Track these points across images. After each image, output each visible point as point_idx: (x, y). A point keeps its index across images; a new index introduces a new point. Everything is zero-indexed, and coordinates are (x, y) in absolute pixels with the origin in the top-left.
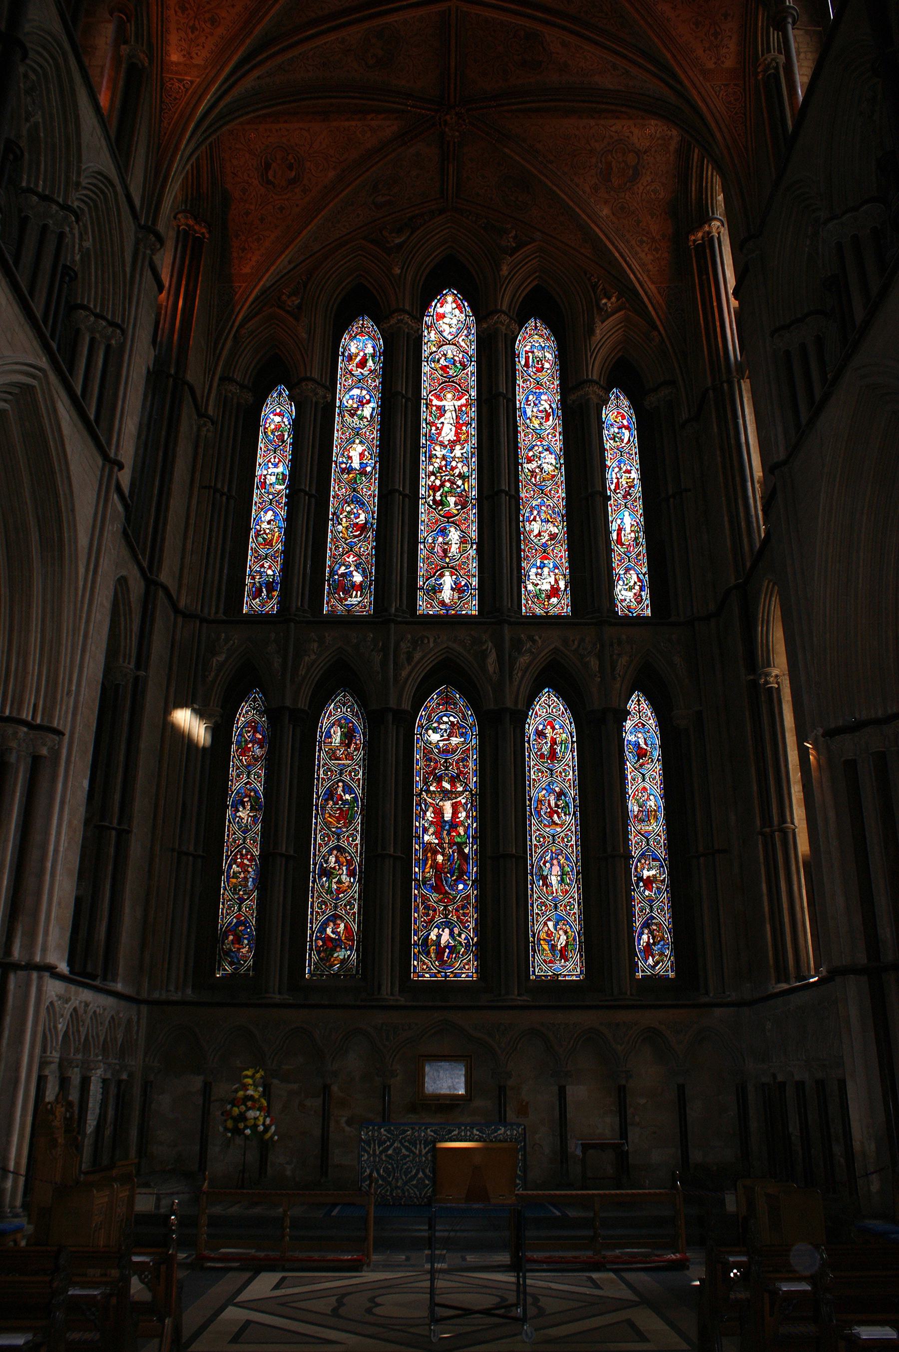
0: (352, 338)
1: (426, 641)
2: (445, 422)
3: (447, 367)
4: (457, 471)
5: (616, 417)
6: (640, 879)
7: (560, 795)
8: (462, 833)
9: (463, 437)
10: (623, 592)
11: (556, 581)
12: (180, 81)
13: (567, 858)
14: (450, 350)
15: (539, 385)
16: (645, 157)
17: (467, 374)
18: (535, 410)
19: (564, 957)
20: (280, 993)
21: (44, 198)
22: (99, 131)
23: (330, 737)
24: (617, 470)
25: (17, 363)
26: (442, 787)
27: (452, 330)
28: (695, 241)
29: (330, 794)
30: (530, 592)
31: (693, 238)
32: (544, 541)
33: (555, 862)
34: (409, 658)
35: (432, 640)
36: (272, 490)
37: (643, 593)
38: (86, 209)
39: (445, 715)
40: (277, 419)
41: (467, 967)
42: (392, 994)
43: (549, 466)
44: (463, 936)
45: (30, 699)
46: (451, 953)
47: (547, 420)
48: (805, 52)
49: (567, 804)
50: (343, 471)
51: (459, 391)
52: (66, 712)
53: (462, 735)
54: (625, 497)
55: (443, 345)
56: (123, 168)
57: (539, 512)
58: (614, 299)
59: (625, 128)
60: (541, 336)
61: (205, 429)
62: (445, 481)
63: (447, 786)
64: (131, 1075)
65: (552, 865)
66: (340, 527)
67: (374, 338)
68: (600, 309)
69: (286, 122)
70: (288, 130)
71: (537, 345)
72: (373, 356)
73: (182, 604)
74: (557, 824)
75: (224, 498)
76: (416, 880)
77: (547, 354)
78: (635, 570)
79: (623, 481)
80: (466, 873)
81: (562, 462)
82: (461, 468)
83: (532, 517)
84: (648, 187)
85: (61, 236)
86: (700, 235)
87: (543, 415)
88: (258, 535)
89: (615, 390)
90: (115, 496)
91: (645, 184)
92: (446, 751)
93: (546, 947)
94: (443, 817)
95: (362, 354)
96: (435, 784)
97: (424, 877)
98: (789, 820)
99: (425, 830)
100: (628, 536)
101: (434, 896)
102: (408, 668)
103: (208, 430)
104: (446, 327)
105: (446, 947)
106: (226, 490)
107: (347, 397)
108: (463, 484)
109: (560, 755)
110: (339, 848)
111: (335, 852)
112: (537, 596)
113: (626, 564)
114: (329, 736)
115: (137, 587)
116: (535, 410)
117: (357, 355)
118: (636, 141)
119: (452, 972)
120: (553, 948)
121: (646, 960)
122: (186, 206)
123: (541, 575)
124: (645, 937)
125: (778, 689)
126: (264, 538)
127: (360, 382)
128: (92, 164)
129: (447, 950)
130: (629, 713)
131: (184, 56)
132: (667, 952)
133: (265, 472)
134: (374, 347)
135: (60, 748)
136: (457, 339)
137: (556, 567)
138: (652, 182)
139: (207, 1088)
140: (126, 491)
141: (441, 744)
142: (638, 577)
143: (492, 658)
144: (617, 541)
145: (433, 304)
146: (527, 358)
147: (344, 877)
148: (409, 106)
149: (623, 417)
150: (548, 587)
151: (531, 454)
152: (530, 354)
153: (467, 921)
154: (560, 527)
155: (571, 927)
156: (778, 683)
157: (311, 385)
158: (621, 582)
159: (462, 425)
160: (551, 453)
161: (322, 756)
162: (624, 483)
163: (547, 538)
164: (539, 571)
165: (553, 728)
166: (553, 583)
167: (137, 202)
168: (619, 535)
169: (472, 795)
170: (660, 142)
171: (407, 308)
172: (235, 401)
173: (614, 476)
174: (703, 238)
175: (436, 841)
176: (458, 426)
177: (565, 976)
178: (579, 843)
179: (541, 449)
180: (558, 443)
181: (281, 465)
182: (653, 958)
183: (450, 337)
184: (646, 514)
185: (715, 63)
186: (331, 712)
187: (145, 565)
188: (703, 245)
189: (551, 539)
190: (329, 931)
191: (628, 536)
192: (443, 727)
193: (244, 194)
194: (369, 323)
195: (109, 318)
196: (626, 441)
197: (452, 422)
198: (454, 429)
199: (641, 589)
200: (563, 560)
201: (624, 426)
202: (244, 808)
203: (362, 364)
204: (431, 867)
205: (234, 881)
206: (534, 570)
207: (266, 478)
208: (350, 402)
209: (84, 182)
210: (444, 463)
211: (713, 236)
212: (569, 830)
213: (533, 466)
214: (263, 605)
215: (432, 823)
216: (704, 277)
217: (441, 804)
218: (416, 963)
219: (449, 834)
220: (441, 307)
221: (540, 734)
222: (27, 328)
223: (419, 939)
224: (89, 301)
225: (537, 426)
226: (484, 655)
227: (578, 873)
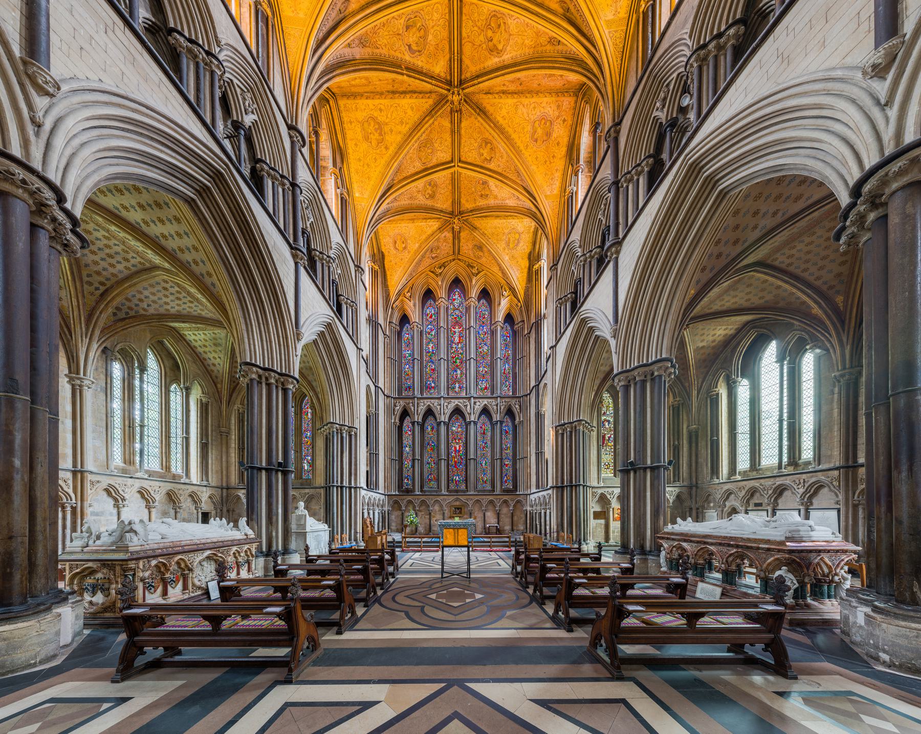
92: (457, 432)
143: (469, 407)
226: (466, 406)
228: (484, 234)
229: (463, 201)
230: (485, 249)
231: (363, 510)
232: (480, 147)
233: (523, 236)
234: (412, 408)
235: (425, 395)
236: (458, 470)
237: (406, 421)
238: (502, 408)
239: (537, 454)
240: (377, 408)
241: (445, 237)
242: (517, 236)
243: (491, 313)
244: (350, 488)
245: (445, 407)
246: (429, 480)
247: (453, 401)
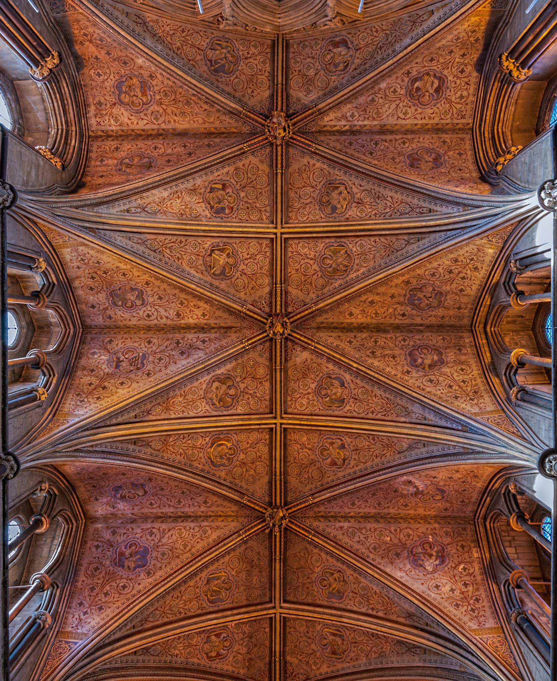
59: (135, 123)
69: (416, 125)
70: (415, 118)
84: (106, 77)
91: (109, 80)
193: (463, 69)
211: (37, 67)
228: (211, 102)
229: (265, 168)
230: (203, 68)
232: (235, 265)
241: (308, 92)
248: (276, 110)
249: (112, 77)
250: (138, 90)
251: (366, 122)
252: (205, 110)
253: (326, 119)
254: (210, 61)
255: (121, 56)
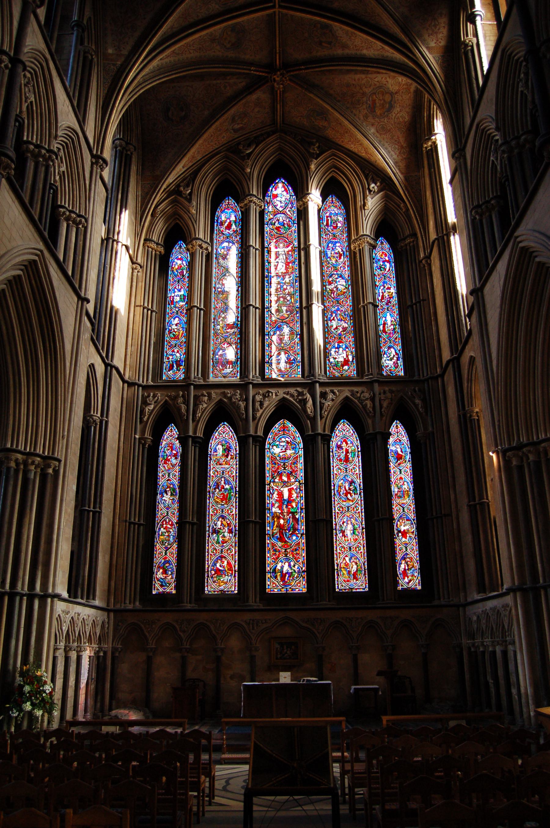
0: (222, 211)
1: (271, 395)
2: (280, 261)
3: (279, 227)
4: (287, 291)
5: (382, 255)
6: (399, 531)
7: (352, 482)
8: (295, 507)
9: (290, 270)
10: (387, 361)
11: (347, 356)
12: (114, 65)
13: (356, 520)
14: (281, 217)
15: (335, 237)
16: (396, 96)
17: (292, 231)
18: (333, 252)
19: (355, 578)
20: (190, 603)
21: (37, 146)
22: (67, 102)
23: (216, 452)
24: (382, 287)
25: (26, 249)
26: (282, 480)
27: (282, 204)
28: (426, 148)
29: (217, 485)
30: (331, 363)
31: (425, 146)
32: (339, 332)
33: (349, 522)
34: (261, 404)
35: (274, 394)
36: (178, 305)
37: (399, 362)
38: (61, 147)
39: (283, 437)
40: (179, 262)
41: (299, 585)
42: (255, 602)
43: (342, 287)
44: (296, 567)
45: (41, 441)
46: (289, 576)
47: (340, 258)
48: (490, 36)
49: (356, 488)
50: (219, 292)
51: (287, 242)
52: (62, 448)
53: (293, 448)
54: (387, 304)
55: (277, 214)
56: (82, 122)
57: (336, 314)
58: (378, 184)
59: (383, 79)
60: (336, 207)
61: (136, 271)
62: (280, 297)
63: (285, 478)
64: (105, 653)
65: (347, 524)
66: (219, 327)
67: (235, 211)
68: (370, 191)
71: (333, 212)
72: (235, 222)
73: (126, 377)
74: (350, 500)
75: (149, 312)
76: (268, 534)
77: (339, 218)
78: (394, 348)
79: (386, 295)
80: (297, 529)
81: (349, 283)
82: (289, 289)
83: (332, 318)
84: (398, 115)
85: (47, 167)
86: (430, 143)
87: (338, 255)
88: (170, 332)
89: (380, 238)
90: (86, 318)
91: (396, 113)
92: (285, 458)
93: (345, 572)
94: (283, 497)
95: (228, 221)
96: (278, 478)
97: (273, 533)
98: (485, 497)
99: (273, 505)
100: (389, 327)
101: (280, 544)
102: (261, 411)
103: (138, 272)
104: (278, 203)
105: (286, 573)
106: (150, 307)
107: (221, 247)
108: (291, 299)
109: (351, 459)
110: (223, 517)
111: (221, 519)
112: (336, 365)
113: (388, 344)
114: (216, 451)
115: (100, 369)
116: (333, 252)
117: (225, 222)
118: (390, 86)
119: (290, 588)
120: (349, 572)
121: (404, 578)
122: (120, 136)
123: (338, 352)
124: (403, 566)
125: (478, 420)
126: (173, 334)
127: (228, 238)
128: (64, 123)
129: (287, 575)
130: (390, 434)
131: (116, 50)
132: (416, 574)
133: (173, 295)
134: (235, 216)
135: (59, 470)
136: (285, 210)
137: (347, 347)
138: (400, 111)
139: (149, 661)
140: (92, 314)
141: (281, 454)
142: (396, 352)
143: (310, 403)
144: (383, 330)
145: (270, 189)
146: (327, 221)
147: (226, 534)
148: (252, 70)
149: (386, 255)
150: (342, 360)
151: (331, 279)
152: (329, 218)
153: (298, 558)
154: (349, 323)
155: (359, 560)
156: (478, 416)
157: (199, 242)
158: (385, 356)
159: (289, 263)
160: (343, 279)
161: (212, 464)
162: (387, 295)
163: (341, 330)
164: (337, 350)
165: (347, 444)
166: (345, 357)
167: (91, 141)
168: (384, 327)
169: (300, 484)
170: (404, 86)
171: (255, 193)
172: (154, 253)
173: (381, 291)
174: (431, 146)
175: (280, 511)
176: (287, 264)
177: (356, 589)
178: (363, 511)
179: (336, 276)
180: (347, 272)
181: (182, 290)
182: (408, 577)
183: (281, 209)
184: (400, 314)
185: (436, 43)
186: (216, 437)
187: (104, 355)
188: (431, 149)
189: (344, 331)
190: (218, 565)
191: (389, 327)
192: (281, 444)
194: (232, 201)
195: (78, 212)
196: (387, 270)
197: (283, 261)
198: (284, 265)
199: (398, 359)
200: (351, 343)
201: (386, 261)
202: (167, 494)
203: (229, 227)
204: (277, 526)
205: (162, 537)
206: (334, 350)
207: (173, 299)
208: (223, 250)
209: (60, 133)
210: (279, 286)
212: (357, 503)
213: (333, 286)
214: (174, 374)
215: (277, 500)
216: (433, 170)
217: (282, 489)
218: (269, 583)
219: (286, 507)
220: (275, 190)
221: (339, 447)
222: (31, 226)
223: (271, 569)
224: (65, 203)
225: (334, 262)
226: (304, 402)
227: (363, 528)
231: (55, 649)
233: (397, 97)
234: (183, 407)
235: (212, 379)
236: (286, 546)
237: (166, 435)
238: (385, 404)
239: (472, 509)
240: (105, 411)
242: (388, 98)
243: (347, 219)
244: (31, 597)
245: (257, 405)
246: (218, 571)
247: (273, 391)
248: (280, 91)
249: (394, 115)
250: (378, 105)
251: (215, 82)
252: (332, 89)
253: (244, 84)
254: (326, 120)
255: (384, 134)
